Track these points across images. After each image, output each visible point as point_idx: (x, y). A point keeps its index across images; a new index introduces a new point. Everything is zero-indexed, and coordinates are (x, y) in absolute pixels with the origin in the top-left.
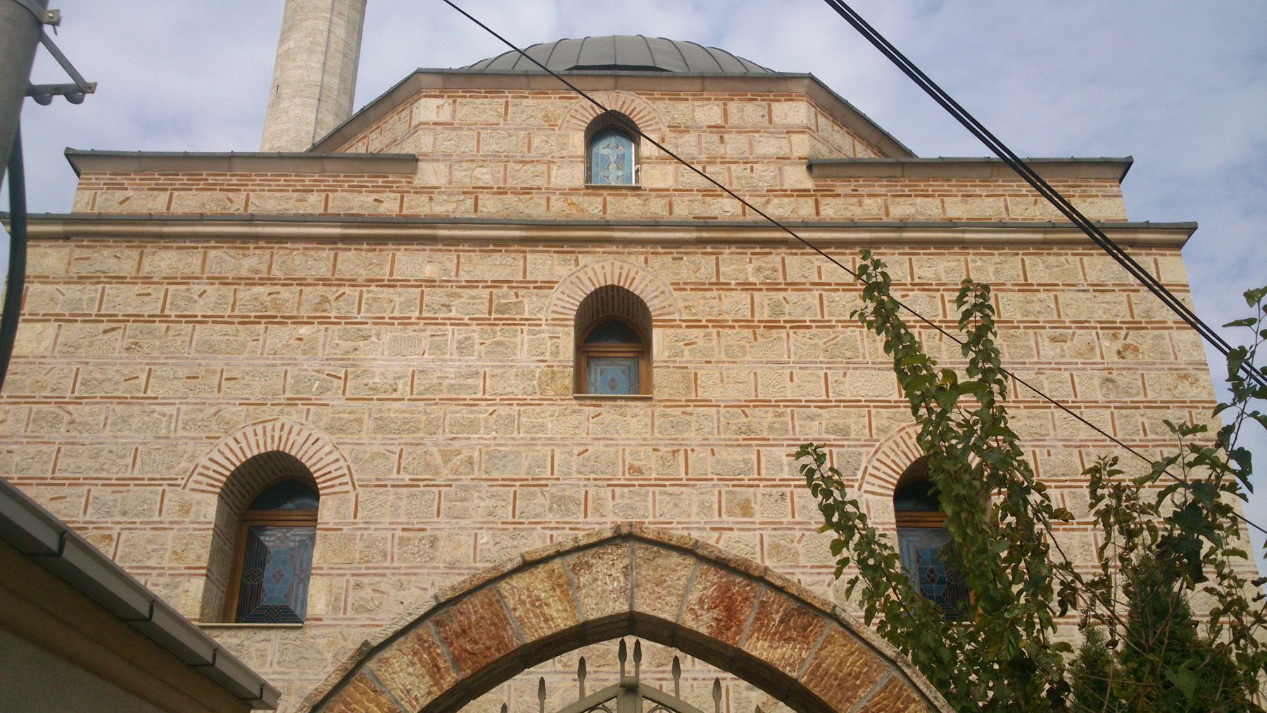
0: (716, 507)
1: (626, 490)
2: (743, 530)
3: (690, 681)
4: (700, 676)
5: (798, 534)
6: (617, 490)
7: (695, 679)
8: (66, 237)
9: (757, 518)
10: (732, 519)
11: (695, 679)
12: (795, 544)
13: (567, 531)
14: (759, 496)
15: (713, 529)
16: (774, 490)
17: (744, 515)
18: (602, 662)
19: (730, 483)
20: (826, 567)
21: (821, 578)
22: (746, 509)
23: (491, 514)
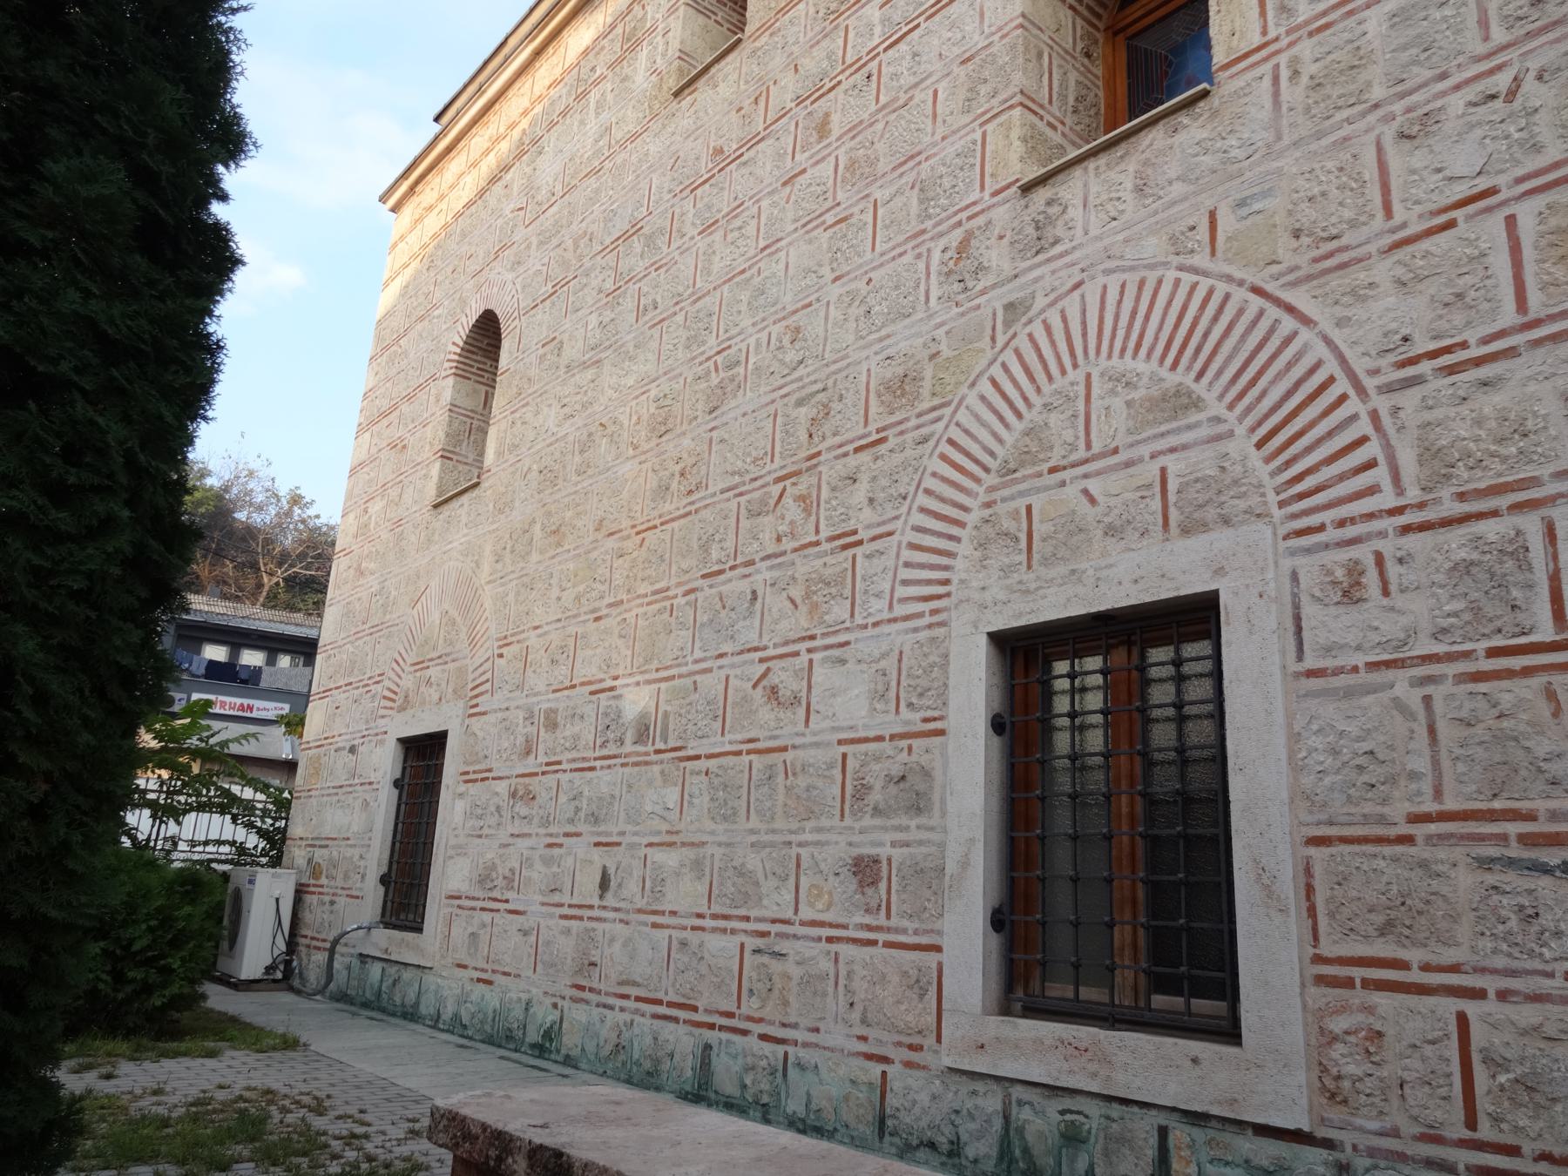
0: (790, 150)
1: (707, 186)
2: (817, 163)
3: (741, 420)
4: (749, 409)
5: (880, 126)
6: (699, 192)
7: (744, 415)
8: (412, 190)
9: (836, 133)
10: (807, 154)
11: (744, 415)
12: (877, 146)
13: (654, 274)
14: (841, 96)
15: (785, 184)
16: (857, 76)
17: (821, 138)
18: (663, 429)
19: (808, 102)
20: (912, 157)
21: (903, 181)
22: (823, 129)
23: (600, 291)
